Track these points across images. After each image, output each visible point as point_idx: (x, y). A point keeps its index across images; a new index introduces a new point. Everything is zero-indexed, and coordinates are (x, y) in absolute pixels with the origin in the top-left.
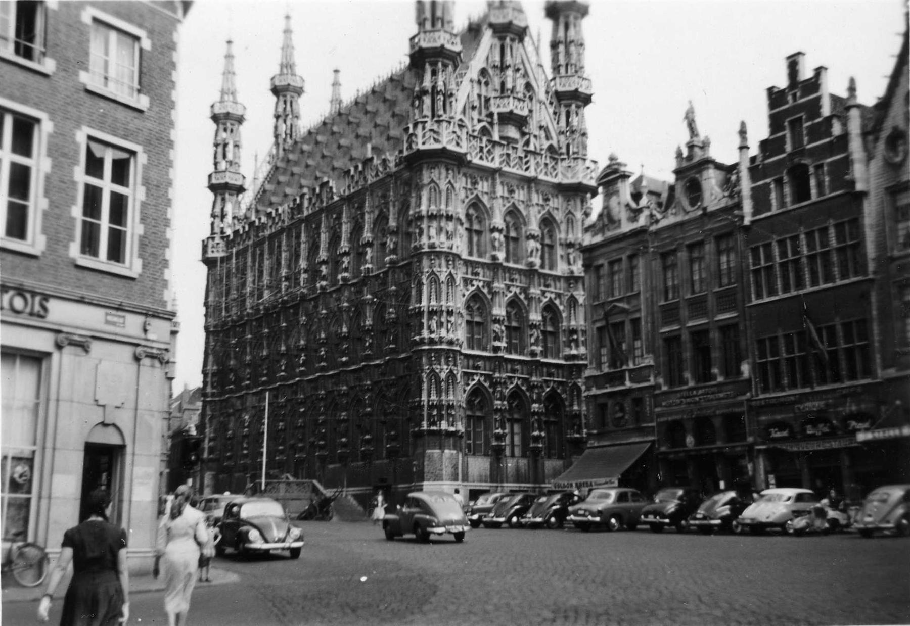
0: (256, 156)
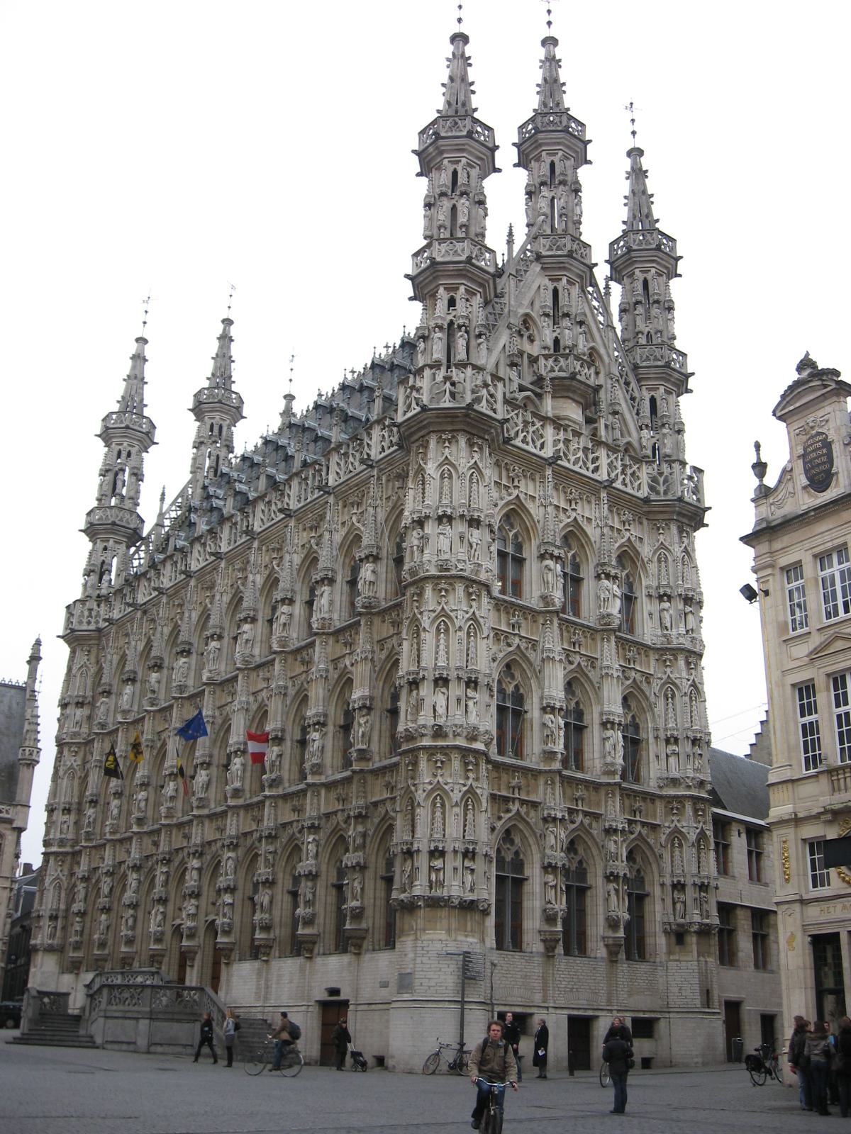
0: (163, 494)
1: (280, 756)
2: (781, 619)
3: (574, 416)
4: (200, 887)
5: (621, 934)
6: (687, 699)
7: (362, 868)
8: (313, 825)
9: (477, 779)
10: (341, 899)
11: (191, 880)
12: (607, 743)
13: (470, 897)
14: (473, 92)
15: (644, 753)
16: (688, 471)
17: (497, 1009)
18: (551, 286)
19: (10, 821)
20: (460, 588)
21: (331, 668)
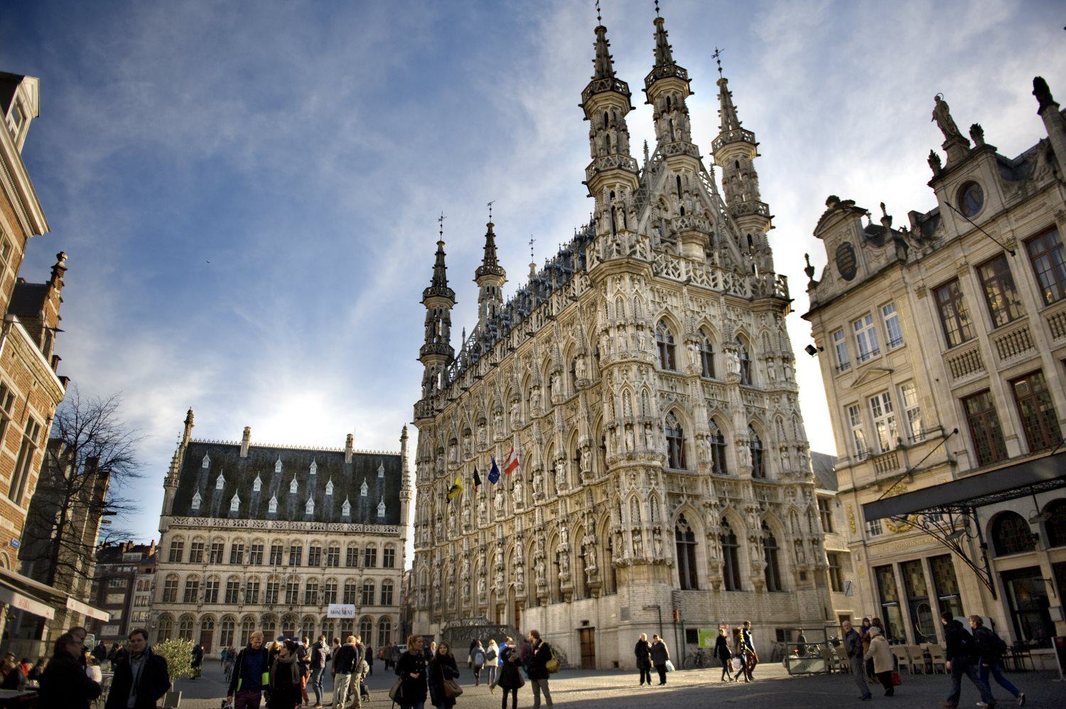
1: (541, 481)
2: (833, 365)
3: (698, 254)
4: (504, 565)
5: (762, 576)
6: (791, 422)
7: (594, 544)
8: (564, 521)
9: (657, 484)
10: (585, 565)
11: (498, 559)
12: (740, 454)
13: (659, 558)
14: (613, 62)
15: (766, 459)
16: (777, 279)
17: (686, 627)
18: (675, 175)
19: (398, 536)
21: (565, 424)
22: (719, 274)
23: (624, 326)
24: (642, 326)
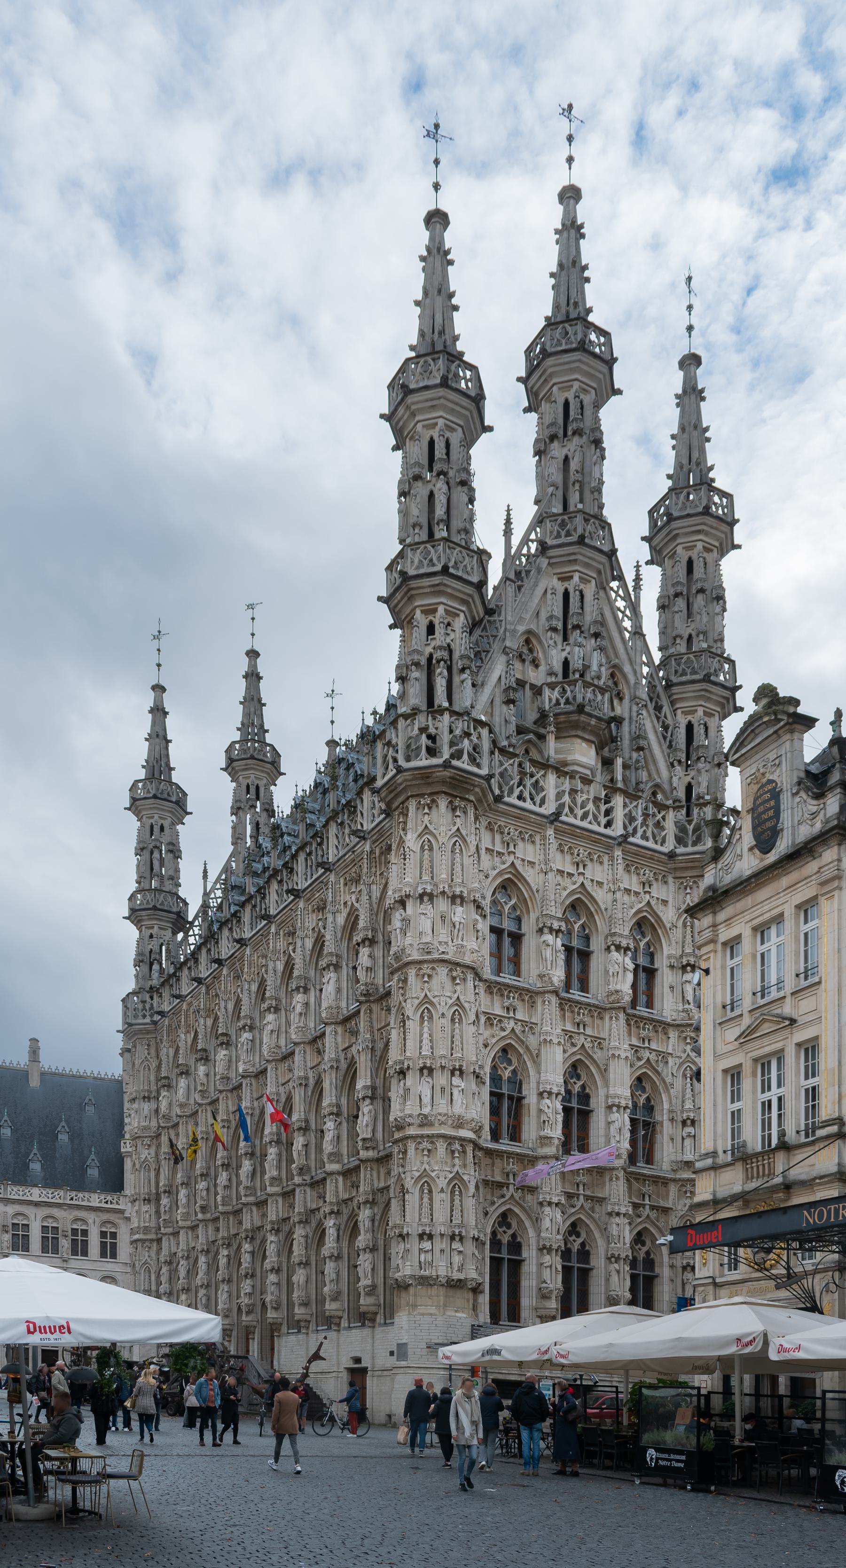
20: (442, 972)
22: (618, 801)
23: (431, 896)
24: (461, 897)
